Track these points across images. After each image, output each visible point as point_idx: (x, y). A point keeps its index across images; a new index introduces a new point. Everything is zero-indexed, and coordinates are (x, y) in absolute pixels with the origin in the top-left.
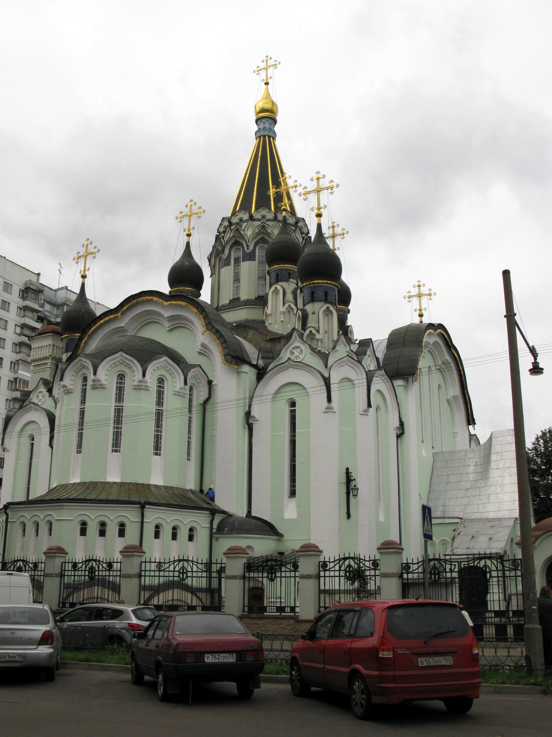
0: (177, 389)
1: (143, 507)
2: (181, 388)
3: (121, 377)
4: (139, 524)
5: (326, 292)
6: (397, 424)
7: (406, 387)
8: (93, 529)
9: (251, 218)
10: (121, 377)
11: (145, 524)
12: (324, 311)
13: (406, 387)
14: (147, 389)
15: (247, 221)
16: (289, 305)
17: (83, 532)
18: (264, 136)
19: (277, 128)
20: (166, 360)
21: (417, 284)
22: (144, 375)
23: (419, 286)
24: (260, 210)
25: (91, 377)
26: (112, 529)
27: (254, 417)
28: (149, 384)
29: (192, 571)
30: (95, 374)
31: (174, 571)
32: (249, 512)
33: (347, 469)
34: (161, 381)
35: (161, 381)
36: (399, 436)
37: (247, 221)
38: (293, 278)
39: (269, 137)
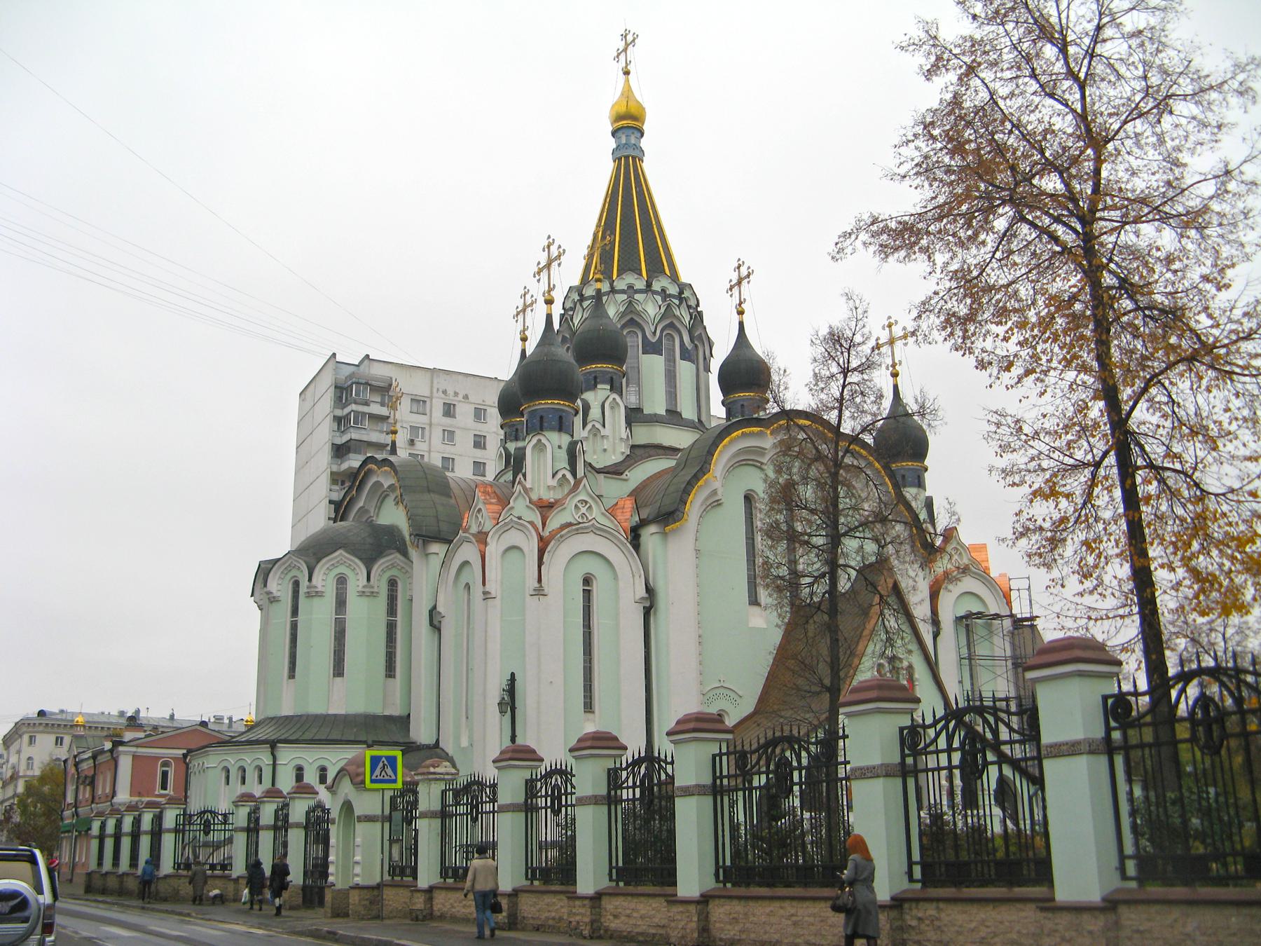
0: (360, 589)
1: (273, 745)
2: (364, 587)
3: (296, 584)
4: (271, 768)
5: (542, 418)
6: (642, 592)
7: (664, 535)
8: (234, 774)
9: (613, 291)
10: (296, 584)
11: (279, 768)
12: (535, 446)
13: (664, 535)
14: (319, 594)
15: (608, 293)
16: (593, 426)
17: (228, 778)
18: (627, 158)
19: (644, 143)
20: (341, 554)
21: (887, 323)
22: (310, 580)
23: (890, 326)
24: (624, 276)
25: (304, 584)
26: (251, 775)
27: (440, 613)
28: (320, 589)
29: (214, 824)
30: (310, 580)
31: (200, 824)
32: (438, 741)
33: (513, 675)
34: (342, 581)
35: (342, 581)
36: (647, 613)
37: (608, 293)
38: (603, 382)
39: (634, 158)
